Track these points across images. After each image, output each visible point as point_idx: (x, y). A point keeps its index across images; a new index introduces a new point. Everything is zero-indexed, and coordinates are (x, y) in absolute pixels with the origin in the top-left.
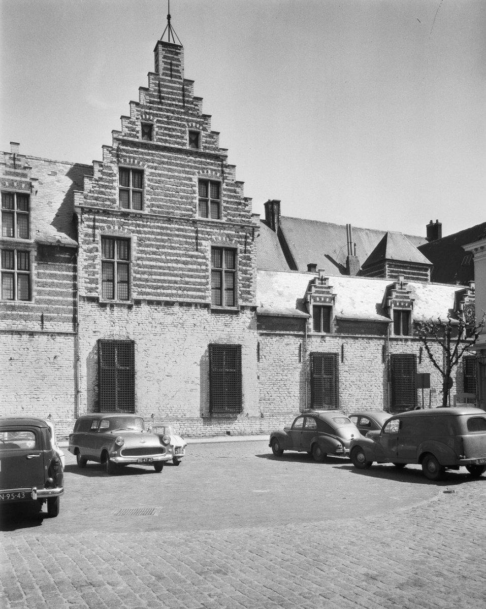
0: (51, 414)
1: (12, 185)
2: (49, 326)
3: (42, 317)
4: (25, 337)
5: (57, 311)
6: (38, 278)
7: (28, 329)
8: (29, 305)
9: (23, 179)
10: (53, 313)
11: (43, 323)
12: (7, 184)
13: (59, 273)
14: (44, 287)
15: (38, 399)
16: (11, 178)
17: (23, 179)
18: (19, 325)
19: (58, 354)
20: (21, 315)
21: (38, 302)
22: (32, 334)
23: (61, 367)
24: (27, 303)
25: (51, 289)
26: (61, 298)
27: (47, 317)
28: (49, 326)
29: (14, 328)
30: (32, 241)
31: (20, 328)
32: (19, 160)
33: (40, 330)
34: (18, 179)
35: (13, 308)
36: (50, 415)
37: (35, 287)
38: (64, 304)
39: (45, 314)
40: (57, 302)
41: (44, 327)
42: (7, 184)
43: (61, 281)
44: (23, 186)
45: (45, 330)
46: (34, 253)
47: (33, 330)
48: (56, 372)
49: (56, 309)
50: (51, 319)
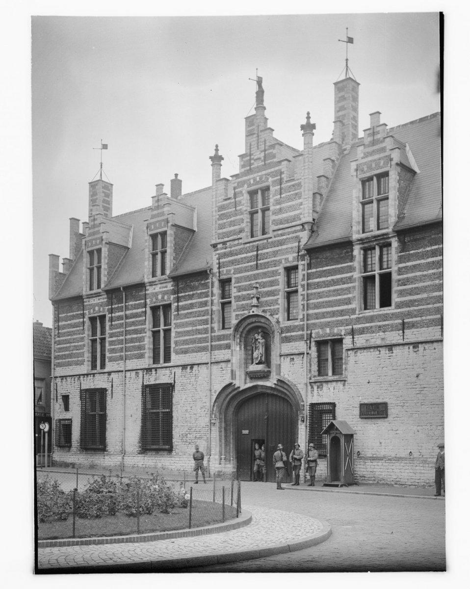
0: (412, 451)
1: (370, 168)
2: (411, 335)
3: (403, 324)
4: (383, 351)
5: (420, 313)
6: (399, 275)
7: (388, 342)
8: (388, 312)
9: (382, 155)
10: (416, 316)
11: (403, 332)
12: (365, 169)
13: (423, 261)
14: (405, 285)
15: (397, 432)
16: (370, 158)
17: (382, 155)
18: (376, 339)
19: (421, 371)
20: (380, 327)
21: (399, 306)
22: (390, 347)
23: (425, 388)
24: (386, 310)
25: (414, 286)
26: (425, 295)
27: (408, 323)
28: (411, 335)
29: (373, 342)
30: (390, 230)
31: (379, 342)
32: (378, 133)
33: (401, 342)
34: (376, 157)
35: (371, 319)
36: (411, 452)
37: (395, 288)
38: (429, 302)
39: (406, 321)
40: (420, 302)
41: (405, 337)
42: (365, 169)
43: (425, 273)
44: (374, 165)
45: (406, 341)
46: (395, 243)
47: (394, 342)
48: (418, 395)
49: (419, 310)
50: (413, 325)
